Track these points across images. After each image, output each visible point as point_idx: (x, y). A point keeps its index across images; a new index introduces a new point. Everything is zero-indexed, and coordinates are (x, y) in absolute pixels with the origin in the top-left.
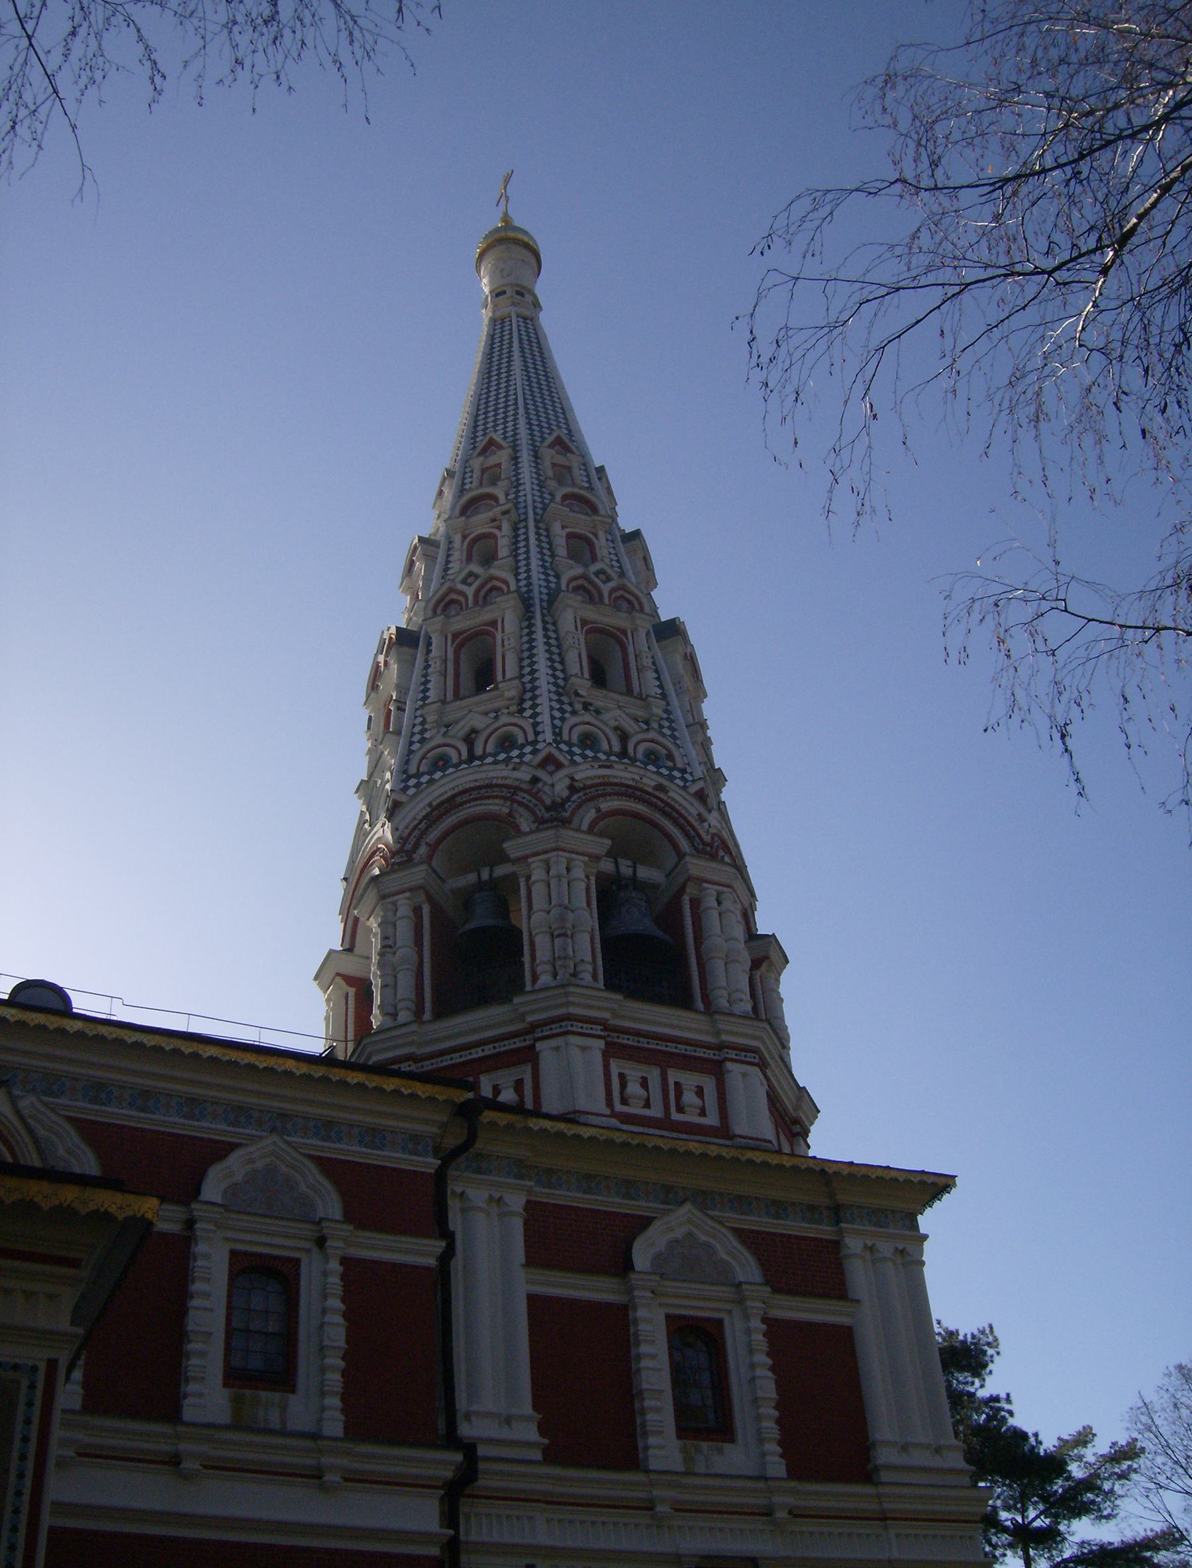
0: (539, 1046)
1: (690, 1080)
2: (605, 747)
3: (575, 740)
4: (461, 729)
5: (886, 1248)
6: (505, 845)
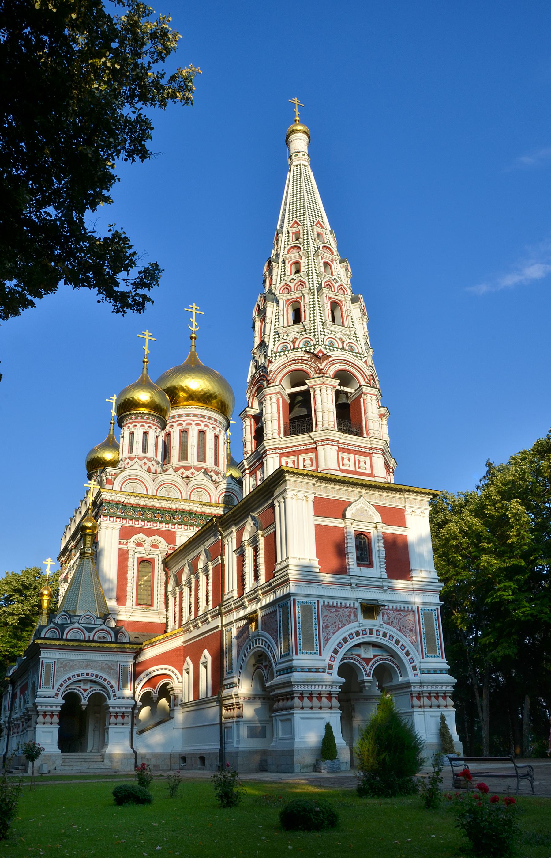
1: (362, 458)
3: (327, 344)
4: (291, 338)
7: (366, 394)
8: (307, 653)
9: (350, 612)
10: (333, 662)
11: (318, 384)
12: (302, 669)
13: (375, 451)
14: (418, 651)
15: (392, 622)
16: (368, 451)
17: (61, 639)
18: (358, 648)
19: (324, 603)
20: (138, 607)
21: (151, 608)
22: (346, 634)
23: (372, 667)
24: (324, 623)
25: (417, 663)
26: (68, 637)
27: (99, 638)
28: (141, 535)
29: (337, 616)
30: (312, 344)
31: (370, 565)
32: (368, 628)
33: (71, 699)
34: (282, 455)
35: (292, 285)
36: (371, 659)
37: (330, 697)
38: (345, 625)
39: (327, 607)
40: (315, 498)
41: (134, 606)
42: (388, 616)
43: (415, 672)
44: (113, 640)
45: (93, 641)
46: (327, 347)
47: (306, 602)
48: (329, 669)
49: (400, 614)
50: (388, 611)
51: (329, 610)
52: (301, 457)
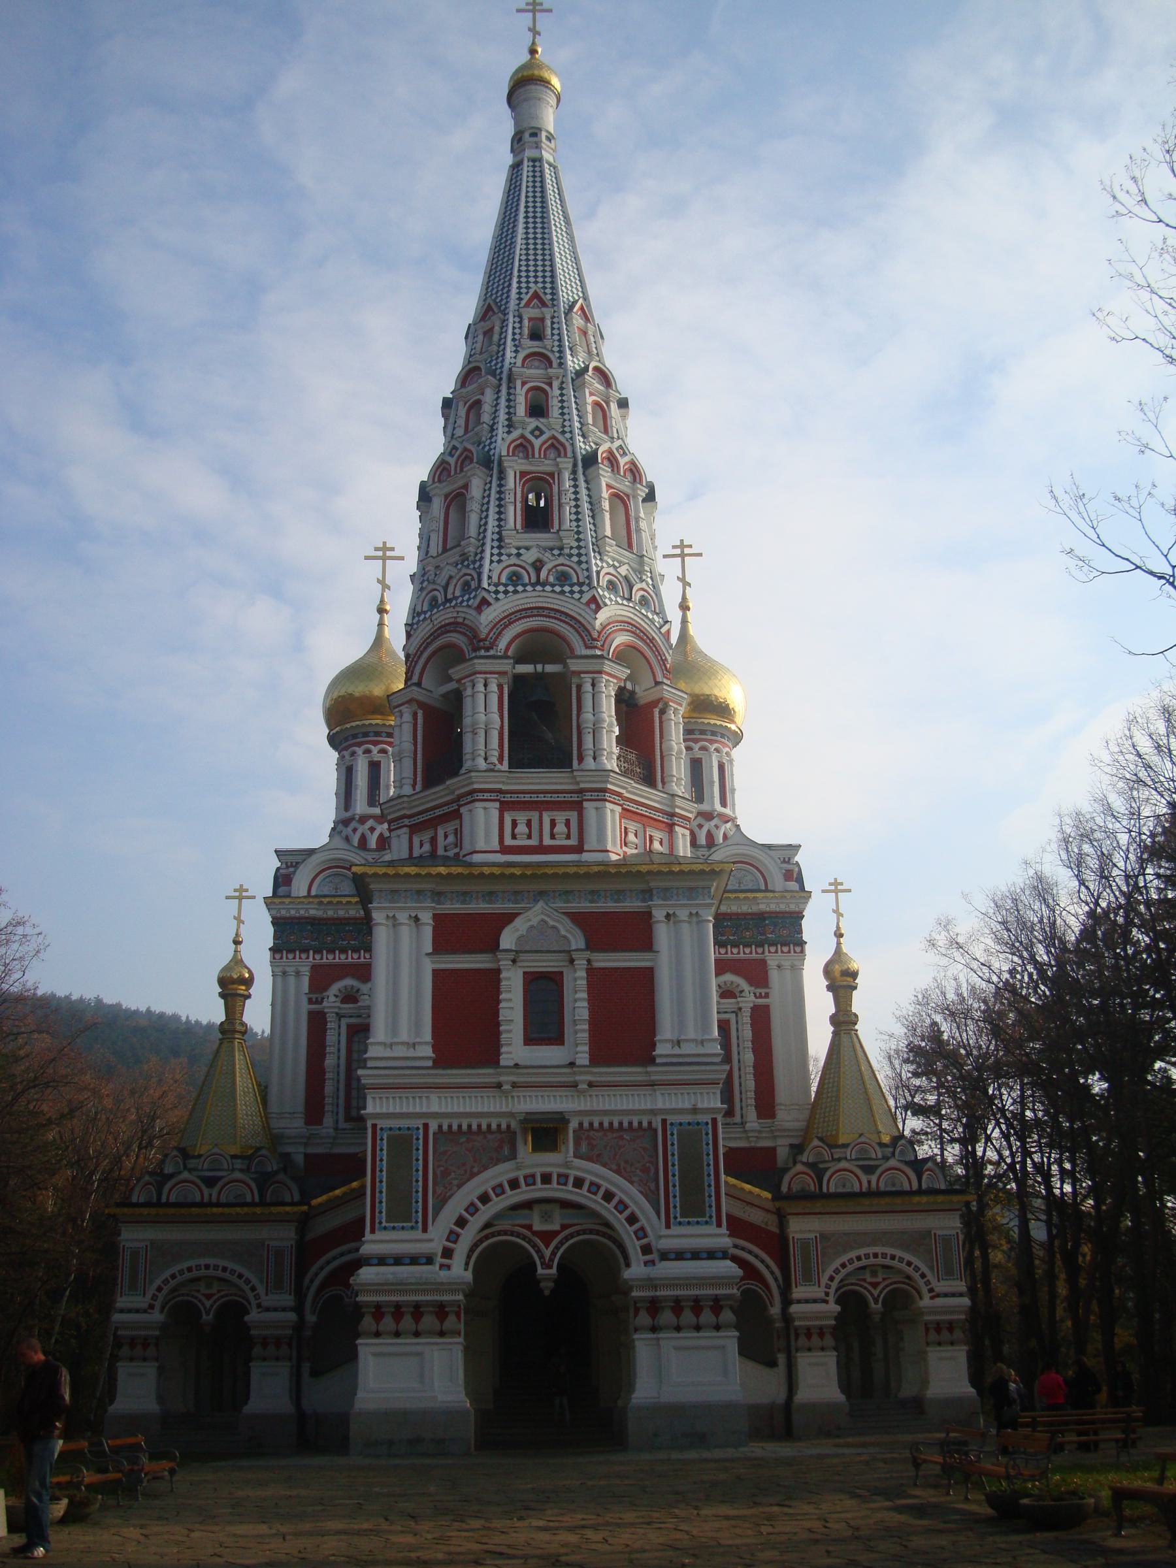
0: (462, 810)
1: (560, 817)
2: (527, 581)
3: (503, 580)
5: (683, 914)
8: (394, 1228)
10: (455, 1242)
12: (382, 1261)
13: (588, 795)
15: (599, 1155)
17: (159, 1204)
18: (526, 1212)
19: (440, 1127)
22: (488, 1187)
23: (557, 1248)
25: (651, 1238)
26: (173, 1199)
28: (349, 982)
31: (559, 1040)
32: (538, 1172)
33: (182, 1313)
34: (414, 829)
35: (452, 461)
36: (556, 1233)
37: (441, 1311)
38: (486, 1168)
40: (436, 917)
41: (342, 1125)
42: (589, 1144)
43: (648, 1257)
44: (257, 1200)
45: (218, 1205)
47: (400, 1129)
49: (621, 1138)
50: (592, 1133)
52: (441, 832)
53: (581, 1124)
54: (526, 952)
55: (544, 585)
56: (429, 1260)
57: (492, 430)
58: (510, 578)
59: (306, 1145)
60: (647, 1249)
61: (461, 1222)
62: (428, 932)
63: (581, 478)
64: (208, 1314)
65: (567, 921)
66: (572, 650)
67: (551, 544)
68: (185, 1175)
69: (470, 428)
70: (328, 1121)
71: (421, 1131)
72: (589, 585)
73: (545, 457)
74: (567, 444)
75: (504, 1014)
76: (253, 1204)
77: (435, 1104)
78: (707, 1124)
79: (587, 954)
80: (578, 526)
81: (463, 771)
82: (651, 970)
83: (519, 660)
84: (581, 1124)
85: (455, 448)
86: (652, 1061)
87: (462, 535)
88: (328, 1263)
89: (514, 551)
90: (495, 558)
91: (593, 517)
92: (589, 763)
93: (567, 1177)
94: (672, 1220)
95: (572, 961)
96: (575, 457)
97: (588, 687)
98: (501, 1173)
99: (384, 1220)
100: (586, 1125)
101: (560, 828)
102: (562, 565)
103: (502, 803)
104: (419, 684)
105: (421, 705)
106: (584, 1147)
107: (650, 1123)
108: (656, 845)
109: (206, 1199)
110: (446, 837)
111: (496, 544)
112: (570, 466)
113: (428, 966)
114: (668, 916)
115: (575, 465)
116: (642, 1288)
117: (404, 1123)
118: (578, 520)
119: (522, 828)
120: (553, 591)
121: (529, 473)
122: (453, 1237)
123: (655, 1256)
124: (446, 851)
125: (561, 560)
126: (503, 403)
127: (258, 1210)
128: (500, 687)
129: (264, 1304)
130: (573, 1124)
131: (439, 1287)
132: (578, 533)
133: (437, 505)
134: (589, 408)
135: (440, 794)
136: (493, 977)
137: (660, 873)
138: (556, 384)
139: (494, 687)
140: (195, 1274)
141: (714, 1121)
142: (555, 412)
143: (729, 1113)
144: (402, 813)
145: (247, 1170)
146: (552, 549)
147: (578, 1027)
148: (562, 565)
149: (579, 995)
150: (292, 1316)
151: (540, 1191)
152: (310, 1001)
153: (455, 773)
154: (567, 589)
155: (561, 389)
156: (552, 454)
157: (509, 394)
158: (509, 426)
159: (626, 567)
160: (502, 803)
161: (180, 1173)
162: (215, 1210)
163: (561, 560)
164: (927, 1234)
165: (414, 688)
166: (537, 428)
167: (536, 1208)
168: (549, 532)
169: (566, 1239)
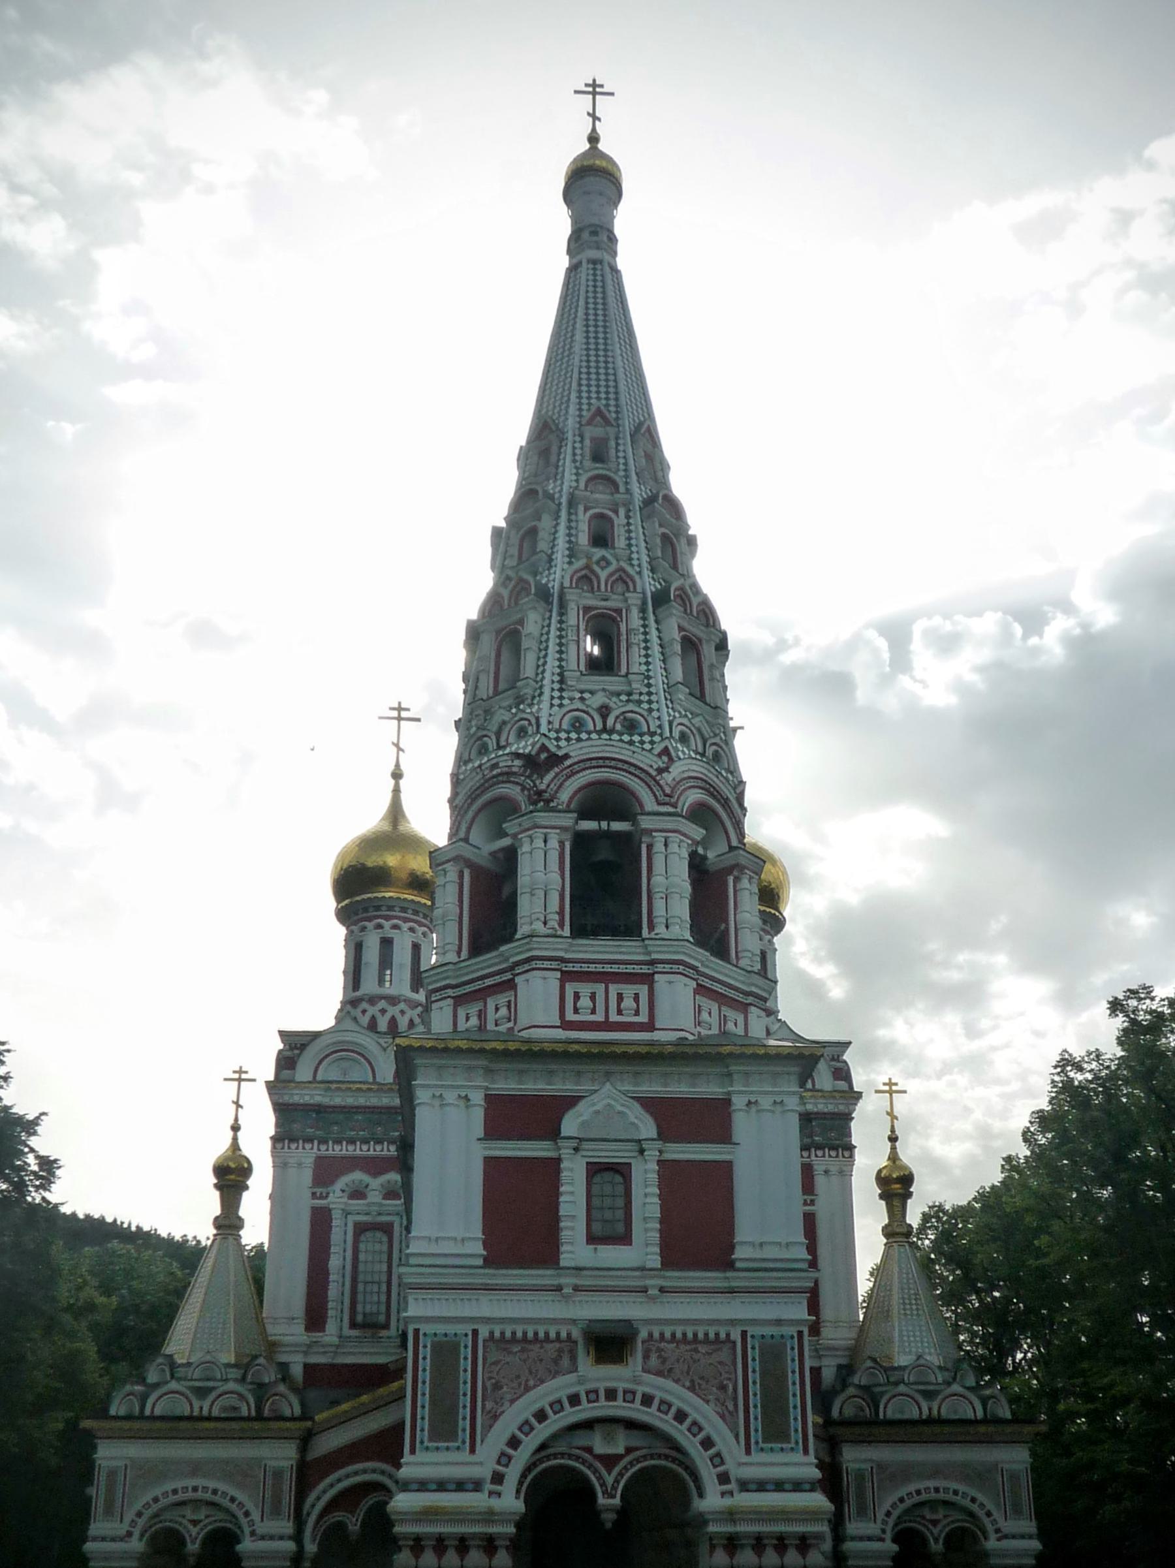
0: (518, 980)
1: (629, 990)
5: (766, 1102)
6: (504, 826)
7: (649, 832)
8: (437, 1449)
9: (560, 1351)
10: (507, 1466)
11: (528, 829)
14: (737, 1437)
15: (670, 1370)
16: (645, 969)
17: (142, 1417)
19: (492, 1333)
20: (355, 1333)
21: (384, 1333)
22: (544, 1403)
23: (621, 1474)
24: (490, 1378)
25: (730, 1466)
26: (157, 1412)
27: (224, 1409)
29: (525, 1361)
30: (530, 732)
31: (625, 1238)
32: (601, 1387)
34: (459, 1001)
38: (542, 1382)
39: (502, 1343)
40: (488, 1098)
41: (347, 1332)
42: (659, 1357)
44: (253, 1413)
46: (563, 735)
48: (492, 1483)
49: (696, 1351)
51: (505, 1349)
52: (491, 1003)
53: (651, 1335)
54: (592, 1140)
55: (611, 732)
56: (477, 1486)
57: (550, 560)
58: (573, 725)
59: (306, 1353)
60: (724, 1478)
61: (514, 1443)
62: (478, 1116)
63: (652, 618)
64: (193, 1542)
65: (636, 1105)
66: (641, 806)
67: (620, 688)
68: (173, 1385)
69: (524, 558)
70: (331, 1327)
71: (470, 1337)
72: (661, 735)
73: (612, 592)
74: (637, 578)
75: (563, 1210)
76: (249, 1419)
77: (487, 1307)
78: (792, 1337)
79: (659, 1144)
80: (648, 670)
81: (517, 936)
82: (730, 1164)
83: (584, 815)
84: (651, 1335)
85: (508, 578)
86: (730, 1265)
87: (516, 678)
88: (332, 1486)
89: (578, 695)
90: (556, 702)
91: (664, 661)
92: (660, 929)
93: (634, 1393)
94: (753, 1447)
95: (642, 1151)
96: (644, 593)
97: (659, 847)
98: (559, 1386)
99: (426, 1439)
100: (656, 1335)
101: (628, 1003)
102: (632, 712)
103: (562, 972)
104: (466, 840)
105: (469, 864)
106: (654, 1361)
107: (728, 1335)
108: (730, 1026)
109: (195, 1414)
110: (497, 1009)
111: (556, 686)
112: (639, 602)
113: (480, 1152)
114: (750, 1103)
115: (644, 603)
116: (715, 1521)
117: (451, 1329)
118: (647, 663)
119: (585, 1002)
120: (621, 741)
121: (597, 608)
122: (504, 1460)
123: (733, 1486)
124: (496, 1025)
125: (631, 707)
126: (562, 530)
127: (257, 1425)
128: (562, 844)
129: (259, 1531)
130: (643, 1334)
131: (489, 1516)
132: (649, 678)
133: (488, 643)
134: (658, 541)
135: (489, 962)
136: (553, 1166)
137: (742, 1056)
138: (622, 512)
139: (554, 843)
140: (180, 1497)
141: (800, 1333)
142: (621, 543)
143: (815, 1329)
144: (447, 982)
145: (243, 1379)
146: (618, 694)
147: (648, 1225)
148: (632, 712)
149: (649, 1190)
150: (291, 1546)
151: (603, 1409)
152: (314, 1194)
153: (510, 939)
154: (636, 738)
155: (628, 517)
156: (620, 588)
157: (570, 521)
158: (570, 556)
159: (700, 718)
160: (562, 972)
161: (167, 1383)
162: (207, 1425)
163: (631, 707)
164: (994, 1466)
165: (461, 843)
166: (603, 558)
167: (597, 1427)
168: (617, 675)
169: (631, 1464)
